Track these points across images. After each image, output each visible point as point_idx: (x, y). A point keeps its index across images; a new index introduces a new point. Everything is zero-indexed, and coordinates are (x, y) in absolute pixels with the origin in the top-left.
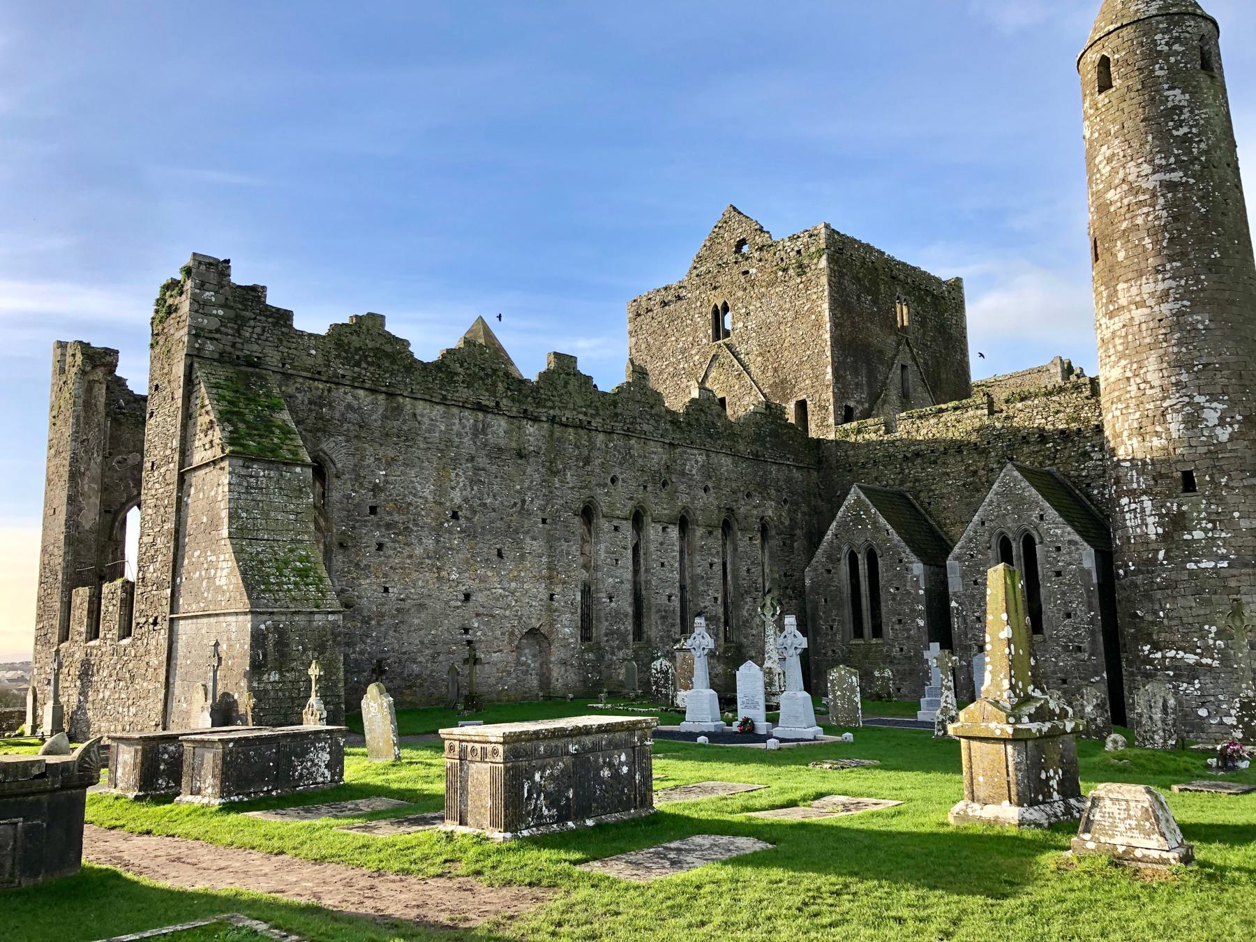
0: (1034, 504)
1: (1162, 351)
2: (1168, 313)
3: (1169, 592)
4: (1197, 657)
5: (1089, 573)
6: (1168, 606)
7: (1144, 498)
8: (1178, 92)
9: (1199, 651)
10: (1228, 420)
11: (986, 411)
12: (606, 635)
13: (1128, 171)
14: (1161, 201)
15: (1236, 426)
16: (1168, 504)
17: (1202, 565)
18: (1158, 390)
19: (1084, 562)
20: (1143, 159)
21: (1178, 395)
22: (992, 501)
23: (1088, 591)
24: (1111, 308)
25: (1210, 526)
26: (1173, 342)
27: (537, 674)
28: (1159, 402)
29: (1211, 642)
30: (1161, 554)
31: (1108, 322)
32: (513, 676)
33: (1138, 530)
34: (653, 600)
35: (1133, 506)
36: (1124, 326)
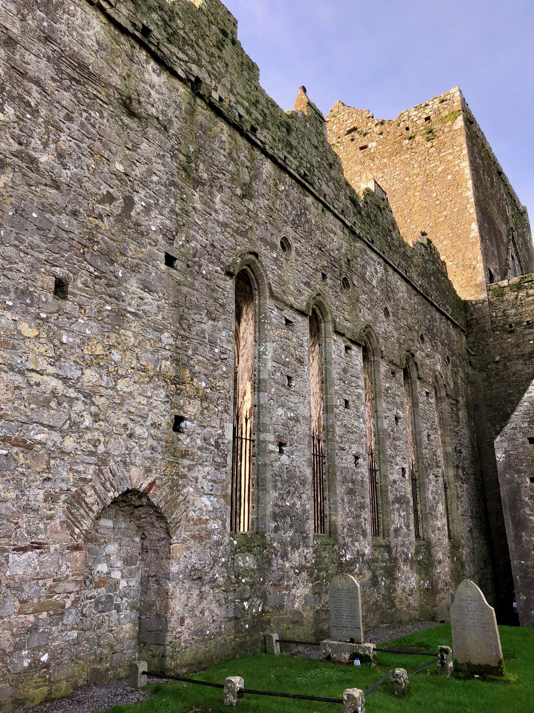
12: (275, 516)
27: (133, 607)
32: (70, 619)
34: (337, 461)
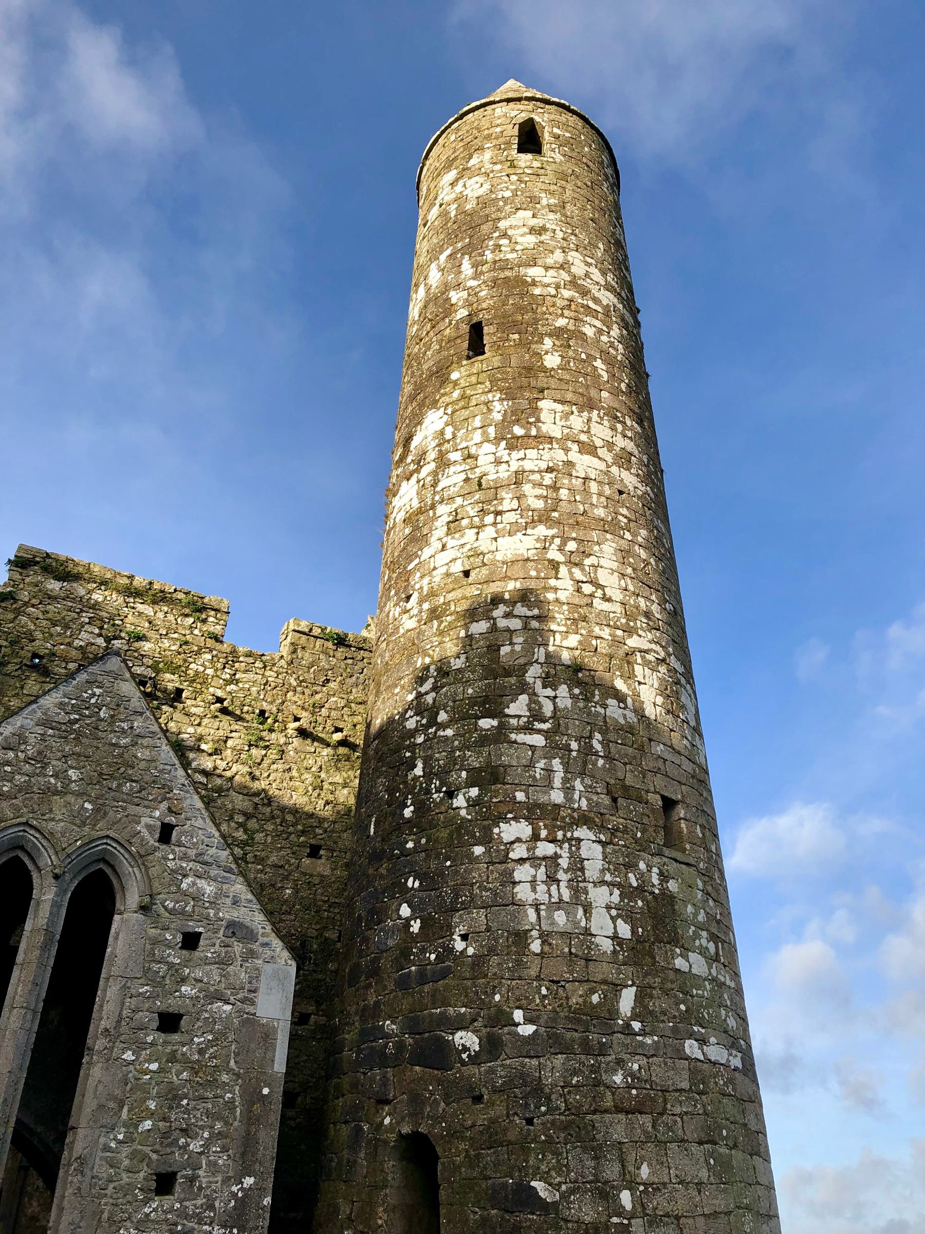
1: (624, 544)
2: (632, 489)
3: (645, 1120)
5: (267, 1036)
6: (645, 1172)
7: (582, 832)
13: (570, 258)
18: (618, 608)
21: (650, 636)
22: (21, 738)
23: (252, 1097)
24: (518, 431)
25: (711, 946)
28: (619, 633)
30: (627, 1000)
31: (502, 452)
33: (560, 917)
35: (545, 849)
36: (550, 470)
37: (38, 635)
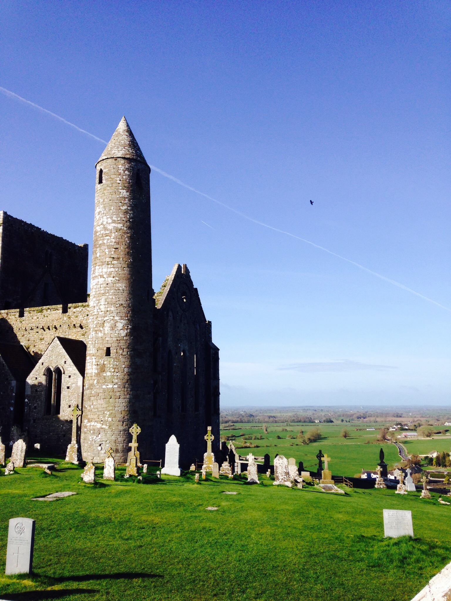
0: (63, 357)
1: (106, 297)
2: (110, 281)
4: (101, 425)
6: (95, 403)
7: (93, 357)
8: (124, 191)
9: (102, 422)
10: (126, 327)
11: (61, 311)
14: (113, 235)
15: (128, 330)
16: (100, 361)
17: (108, 387)
19: (78, 383)
20: (109, 216)
21: (109, 316)
22: (47, 354)
23: (78, 396)
26: (111, 294)
28: (103, 318)
29: (106, 418)
36: (96, 284)
37: (74, 321)
